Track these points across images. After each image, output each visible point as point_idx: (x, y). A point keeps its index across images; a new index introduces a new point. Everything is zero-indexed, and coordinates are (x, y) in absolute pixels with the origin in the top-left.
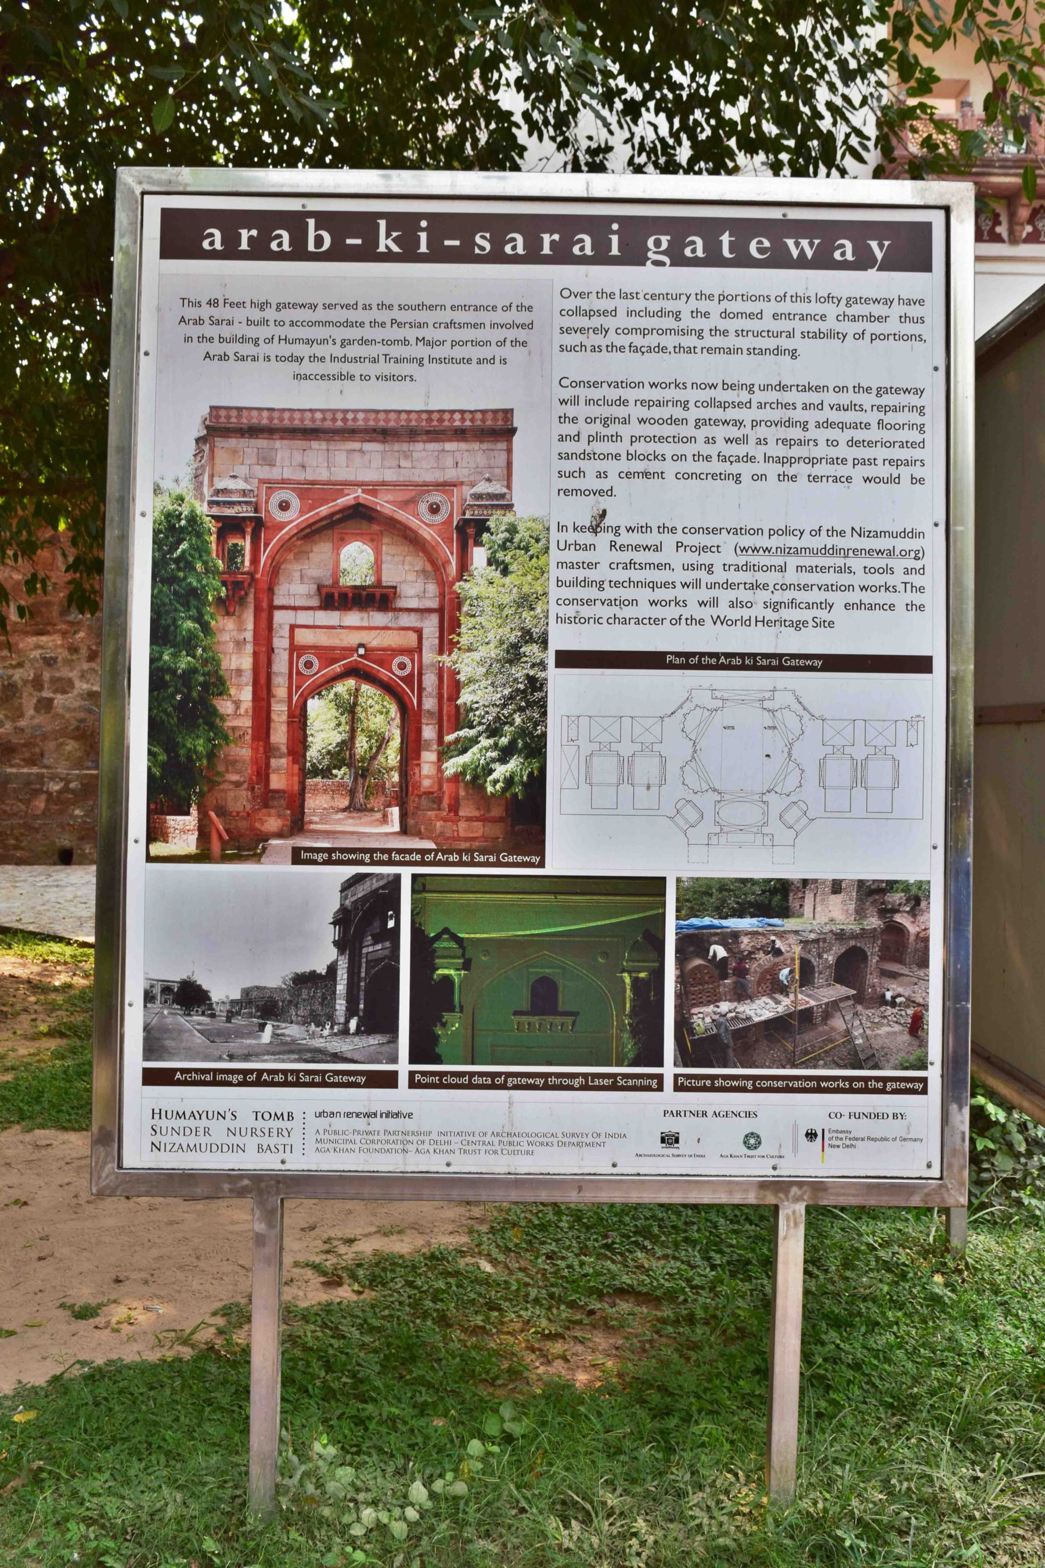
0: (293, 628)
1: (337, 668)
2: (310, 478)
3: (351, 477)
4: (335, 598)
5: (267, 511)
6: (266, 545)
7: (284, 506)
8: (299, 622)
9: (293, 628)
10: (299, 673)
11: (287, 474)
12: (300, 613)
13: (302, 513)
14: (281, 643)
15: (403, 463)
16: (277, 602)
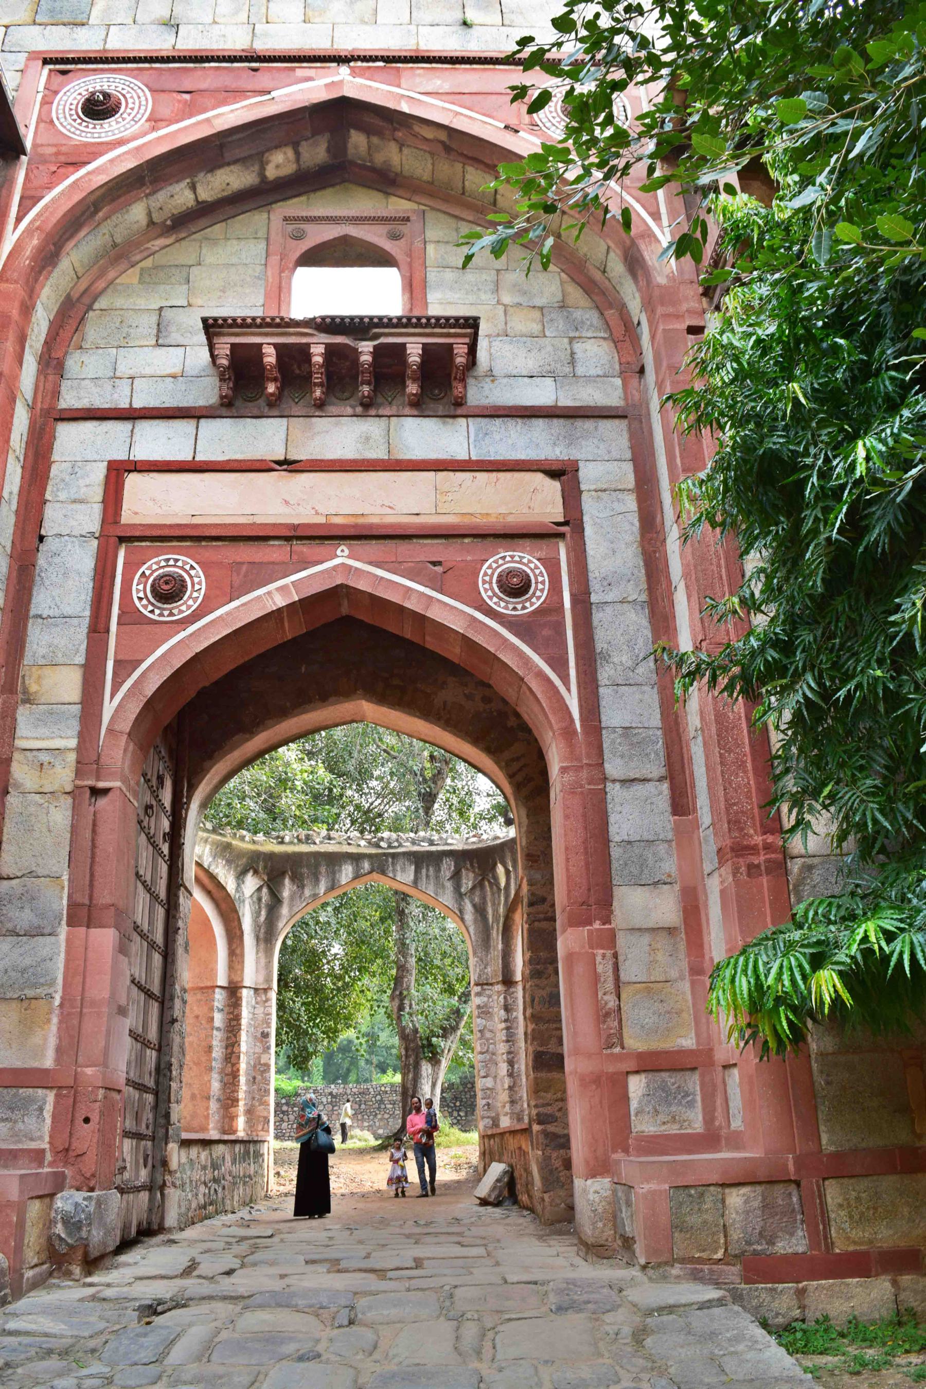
0: (118, 471)
1: (273, 596)
2: (189, 42)
3: (319, 43)
4: (262, 373)
5: (46, 121)
6: (29, 200)
7: (98, 108)
8: (141, 453)
9: (118, 471)
10: (130, 616)
11: (120, 41)
12: (145, 428)
13: (155, 121)
14: (73, 517)
15: (471, 16)
16: (69, 400)
